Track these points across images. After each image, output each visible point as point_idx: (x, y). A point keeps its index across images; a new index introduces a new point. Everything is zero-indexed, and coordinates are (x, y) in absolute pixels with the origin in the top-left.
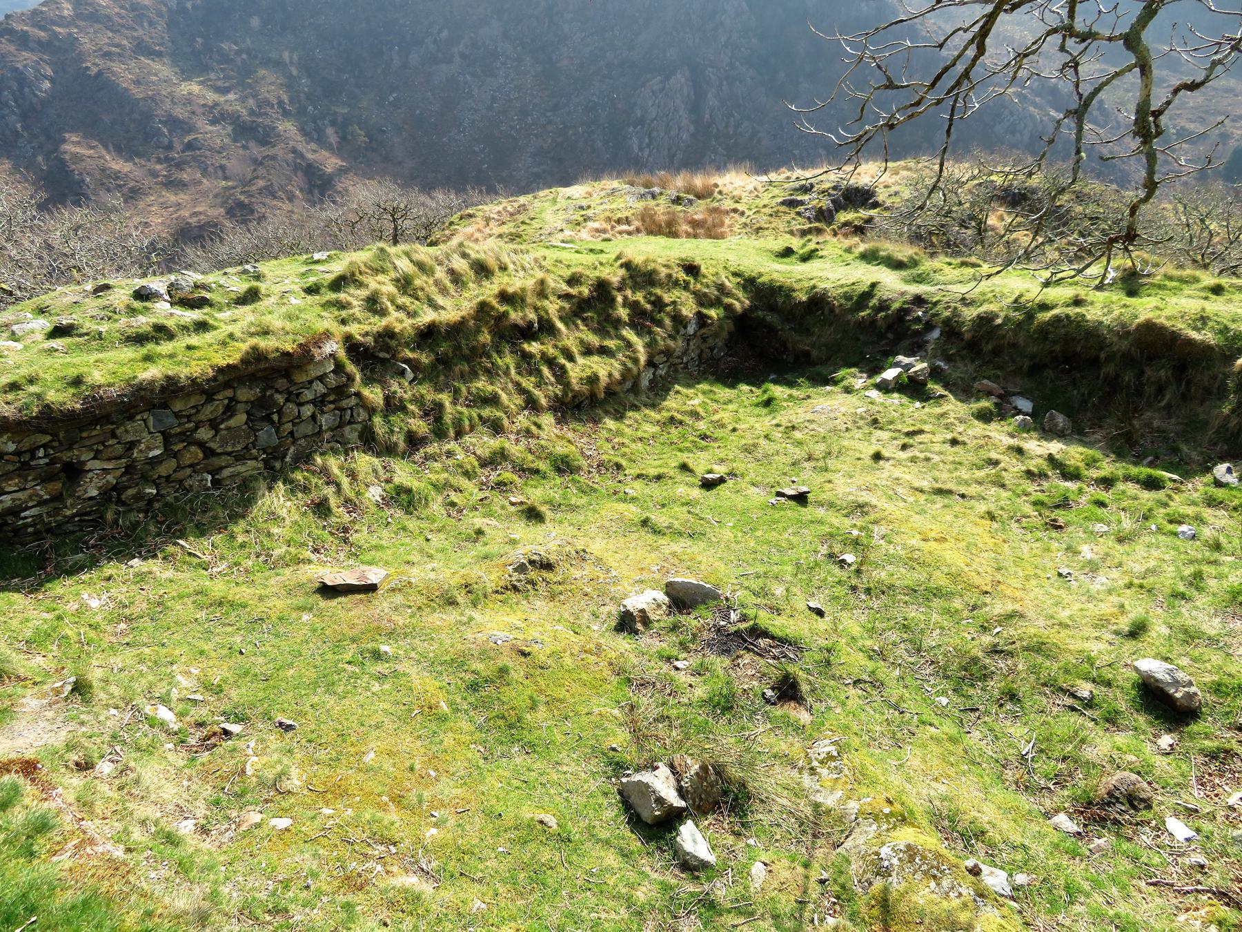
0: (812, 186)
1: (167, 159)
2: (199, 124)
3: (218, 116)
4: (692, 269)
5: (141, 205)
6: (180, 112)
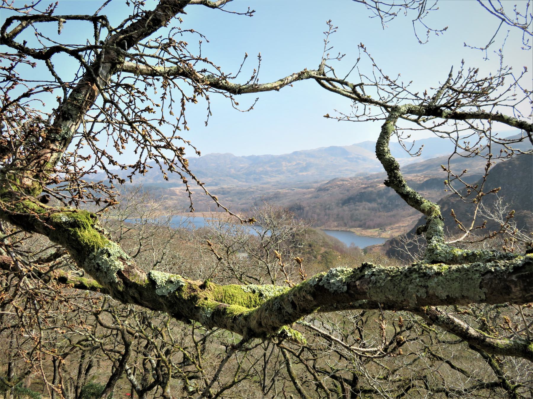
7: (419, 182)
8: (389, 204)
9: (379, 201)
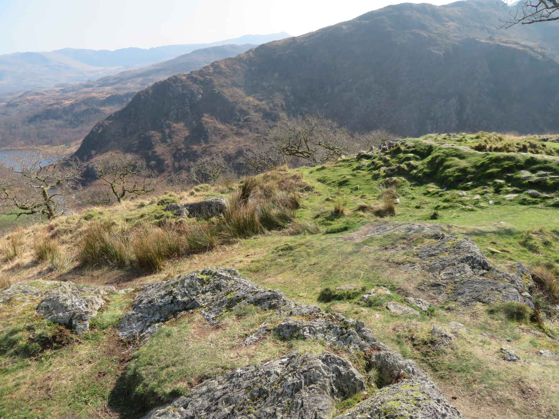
0: (548, 139)
1: (238, 125)
2: (251, 112)
3: (258, 109)
4: (544, 146)
5: (226, 141)
6: (245, 108)
7: (101, 99)
8: (75, 120)
9: (65, 118)
